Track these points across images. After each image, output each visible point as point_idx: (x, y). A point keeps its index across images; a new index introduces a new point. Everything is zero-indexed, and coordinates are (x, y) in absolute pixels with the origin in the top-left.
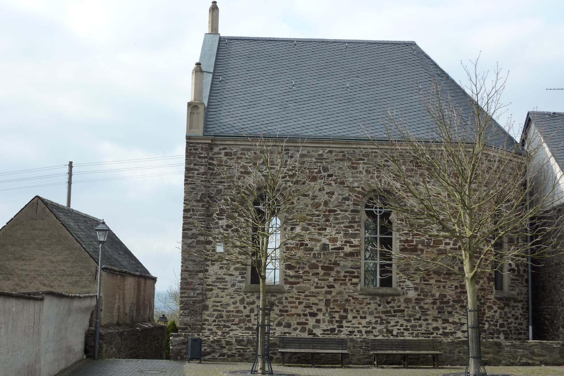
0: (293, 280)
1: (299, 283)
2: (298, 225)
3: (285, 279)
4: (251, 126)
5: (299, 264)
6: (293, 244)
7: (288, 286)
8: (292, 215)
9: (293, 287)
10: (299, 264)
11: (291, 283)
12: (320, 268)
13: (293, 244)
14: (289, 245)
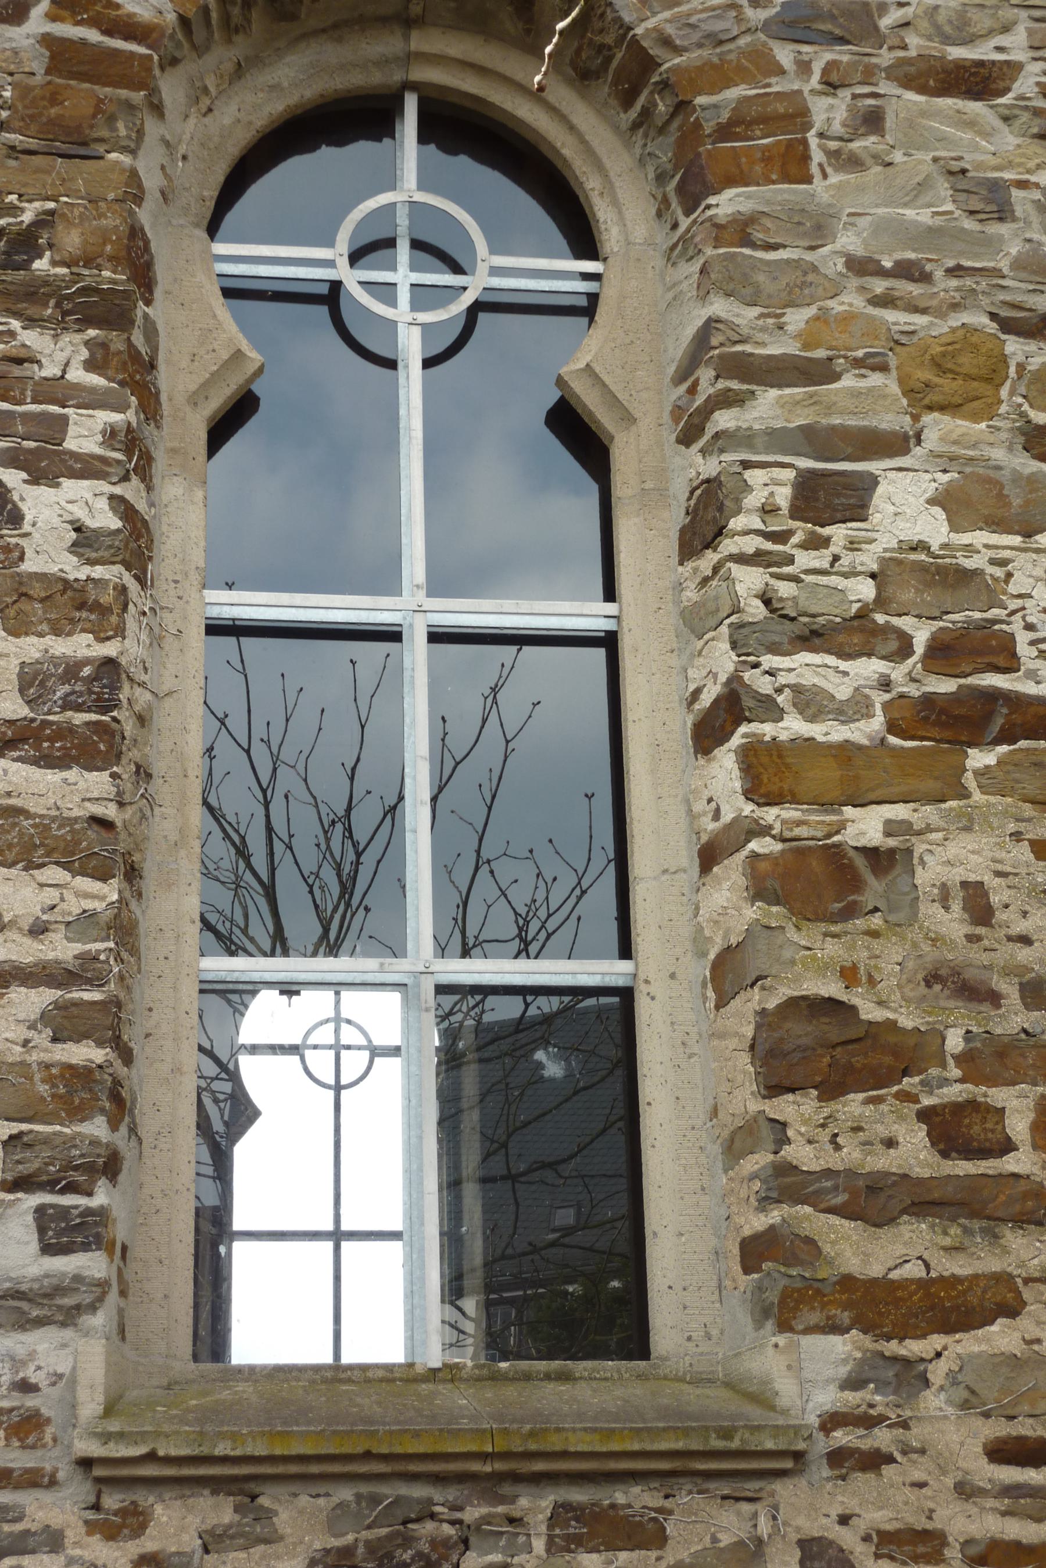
0: (900, 1252)
1: (1001, 1300)
2: (895, 445)
3: (755, 1251)
4: (57, 485)
5: (976, 993)
6: (855, 708)
7: (836, 1351)
8: (797, 319)
9: (911, 1376)
10: (976, 993)
11: (877, 1307)
12: (1019, 1125)
13: (855, 708)
14: (793, 726)
